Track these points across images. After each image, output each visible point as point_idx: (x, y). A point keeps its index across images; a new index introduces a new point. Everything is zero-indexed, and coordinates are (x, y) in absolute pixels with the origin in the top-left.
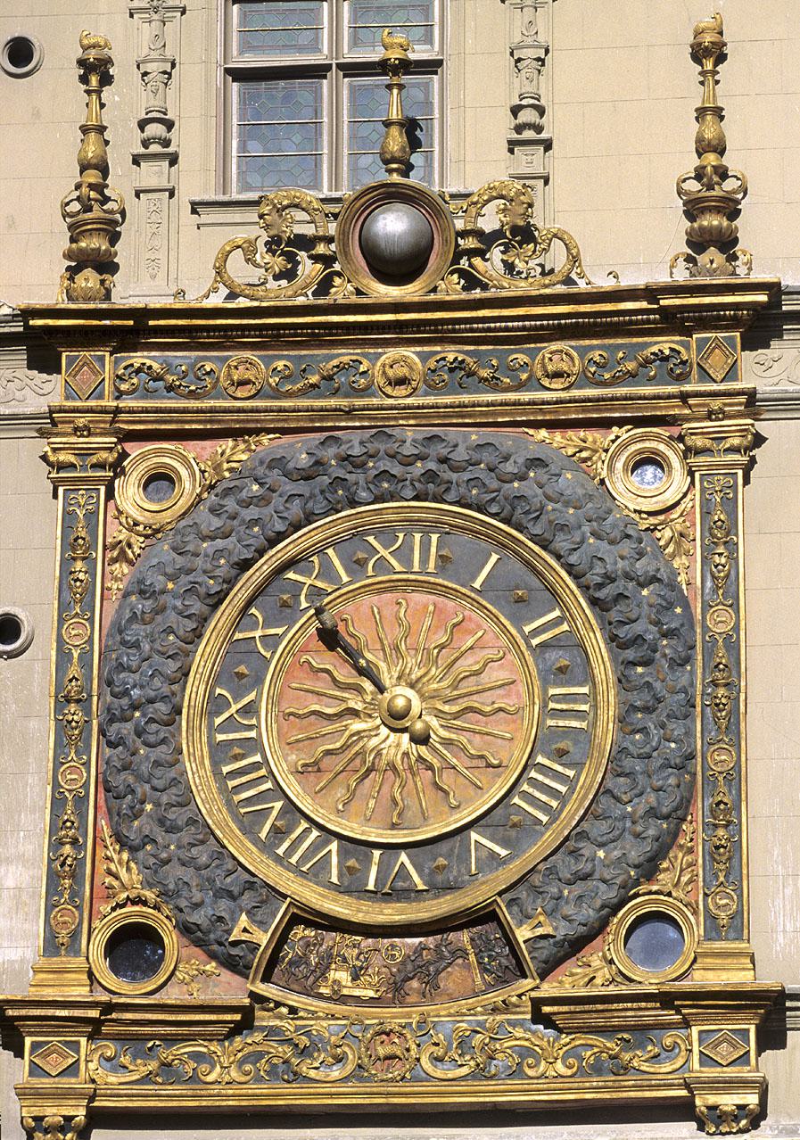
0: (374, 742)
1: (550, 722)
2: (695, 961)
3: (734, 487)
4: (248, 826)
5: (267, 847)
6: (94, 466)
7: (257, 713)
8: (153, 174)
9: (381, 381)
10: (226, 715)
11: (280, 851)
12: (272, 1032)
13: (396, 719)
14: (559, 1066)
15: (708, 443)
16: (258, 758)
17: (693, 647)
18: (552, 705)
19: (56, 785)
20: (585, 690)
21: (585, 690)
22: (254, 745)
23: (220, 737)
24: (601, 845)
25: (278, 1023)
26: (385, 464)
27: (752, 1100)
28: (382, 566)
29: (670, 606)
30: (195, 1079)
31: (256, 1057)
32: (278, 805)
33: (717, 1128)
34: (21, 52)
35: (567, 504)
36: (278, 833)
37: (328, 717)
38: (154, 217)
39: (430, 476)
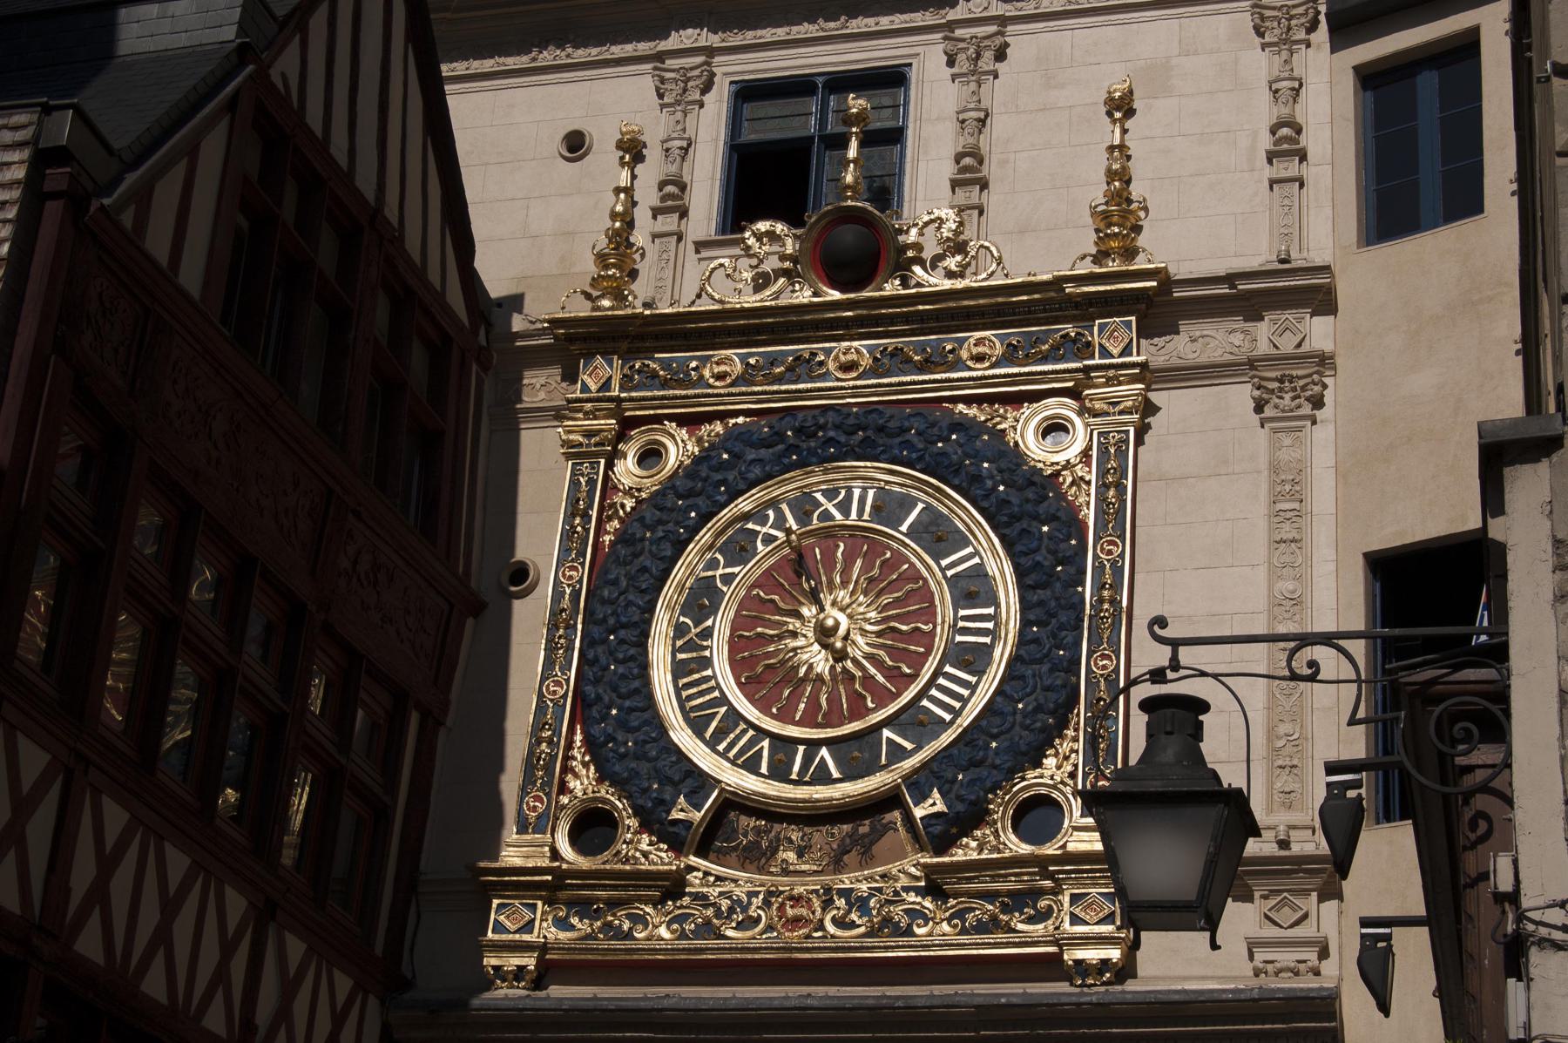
0: (805, 657)
1: (959, 638)
3: (1127, 441)
4: (697, 726)
5: (712, 744)
6: (596, 445)
7: (711, 636)
8: (669, 222)
9: (831, 365)
11: (721, 748)
12: (696, 897)
13: (824, 634)
14: (945, 927)
15: (1106, 407)
16: (709, 672)
18: (961, 624)
19: (540, 695)
20: (991, 611)
21: (991, 611)
22: (707, 663)
23: (680, 656)
24: (994, 737)
25: (705, 890)
26: (831, 434)
27: (1115, 954)
28: (826, 516)
29: (1069, 538)
30: (629, 935)
34: (576, 144)
36: (720, 734)
38: (665, 256)
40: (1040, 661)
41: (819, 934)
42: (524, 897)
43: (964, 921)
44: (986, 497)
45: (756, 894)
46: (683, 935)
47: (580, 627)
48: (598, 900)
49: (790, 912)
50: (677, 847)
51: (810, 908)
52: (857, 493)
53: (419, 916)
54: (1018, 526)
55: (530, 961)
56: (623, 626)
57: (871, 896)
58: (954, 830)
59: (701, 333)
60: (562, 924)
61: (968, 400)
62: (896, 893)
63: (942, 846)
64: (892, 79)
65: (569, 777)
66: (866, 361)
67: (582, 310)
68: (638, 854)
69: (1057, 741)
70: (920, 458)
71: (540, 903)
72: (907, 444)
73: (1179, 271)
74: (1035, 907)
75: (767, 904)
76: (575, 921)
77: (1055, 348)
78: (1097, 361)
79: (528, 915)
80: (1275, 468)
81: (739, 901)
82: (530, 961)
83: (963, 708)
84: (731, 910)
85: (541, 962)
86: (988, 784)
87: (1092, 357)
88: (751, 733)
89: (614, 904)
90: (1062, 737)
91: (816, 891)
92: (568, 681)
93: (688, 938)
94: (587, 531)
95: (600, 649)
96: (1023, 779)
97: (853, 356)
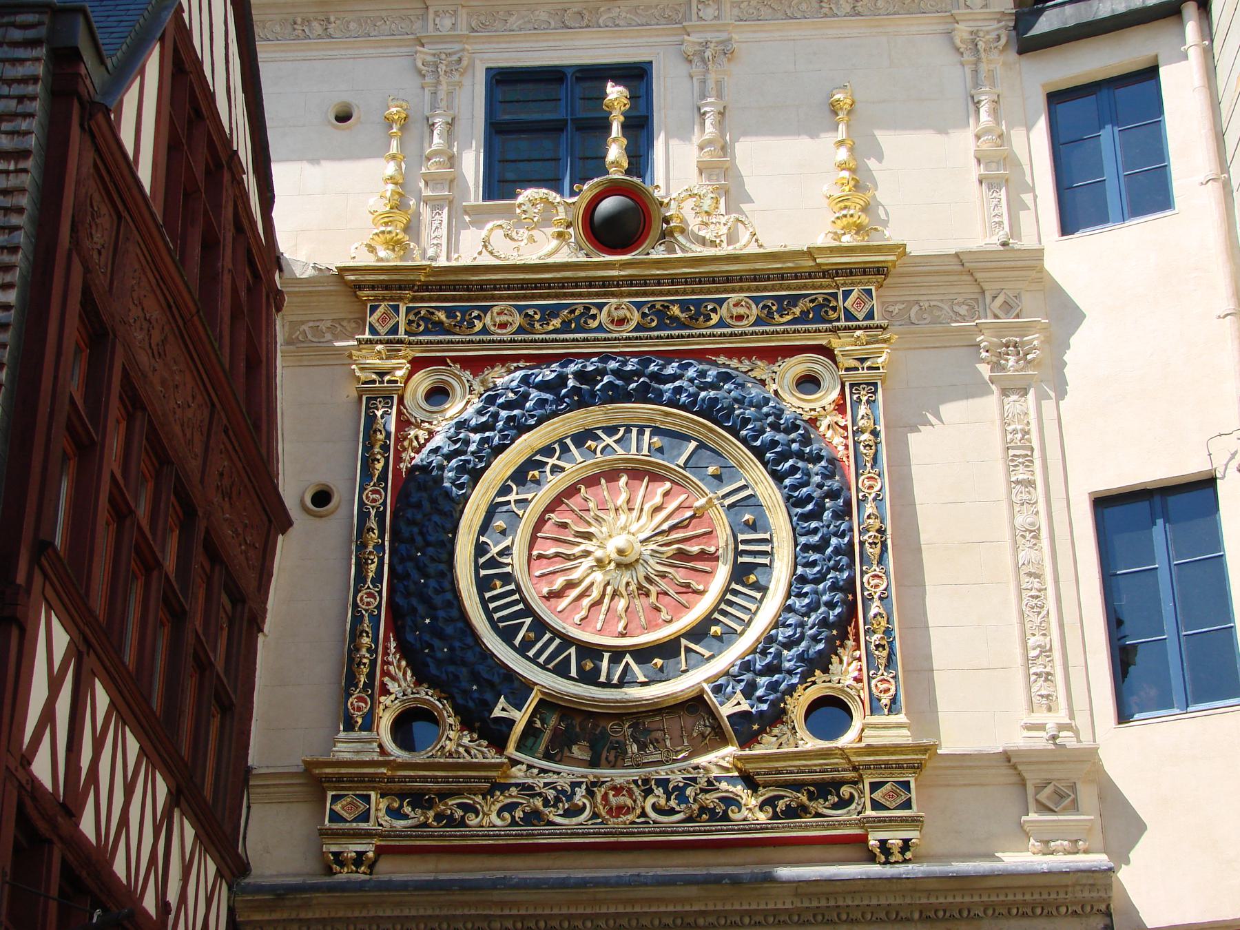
2: (863, 730)
4: (507, 635)
5: (522, 650)
10: (488, 556)
11: (531, 654)
16: (513, 587)
17: (848, 503)
18: (741, 547)
19: (355, 605)
23: (483, 572)
25: (530, 781)
30: (462, 823)
31: (510, 808)
32: (528, 621)
33: (887, 858)
35: (751, 405)
37: (568, 558)
39: (645, 388)
40: (816, 581)
41: (642, 820)
42: (357, 789)
43: (774, 807)
44: (755, 438)
45: (579, 784)
46: (514, 823)
47: (387, 544)
48: (429, 791)
49: (614, 801)
50: (499, 743)
51: (631, 797)
52: (635, 430)
53: (249, 807)
54: (787, 465)
55: (368, 848)
56: (428, 544)
57: (687, 785)
58: (756, 727)
59: (482, 286)
60: (395, 813)
61: (730, 353)
62: (709, 782)
63: (747, 740)
64: (637, 76)
65: (386, 679)
66: (636, 317)
67: (367, 260)
68: (461, 750)
69: (840, 650)
70: (694, 403)
71: (373, 794)
72: (679, 390)
73: (914, 249)
74: (838, 795)
75: (590, 793)
76: (407, 810)
77: (804, 313)
78: (843, 323)
79: (362, 806)
80: (1005, 421)
81: (563, 792)
82: (368, 848)
83: (751, 620)
84: (557, 800)
85: (380, 851)
86: (783, 687)
87: (838, 320)
88: (557, 641)
89: (444, 795)
90: (843, 646)
91: (635, 782)
92: (380, 593)
93: (517, 824)
94: (387, 459)
95: (410, 565)
96: (814, 683)
97: (622, 313)
